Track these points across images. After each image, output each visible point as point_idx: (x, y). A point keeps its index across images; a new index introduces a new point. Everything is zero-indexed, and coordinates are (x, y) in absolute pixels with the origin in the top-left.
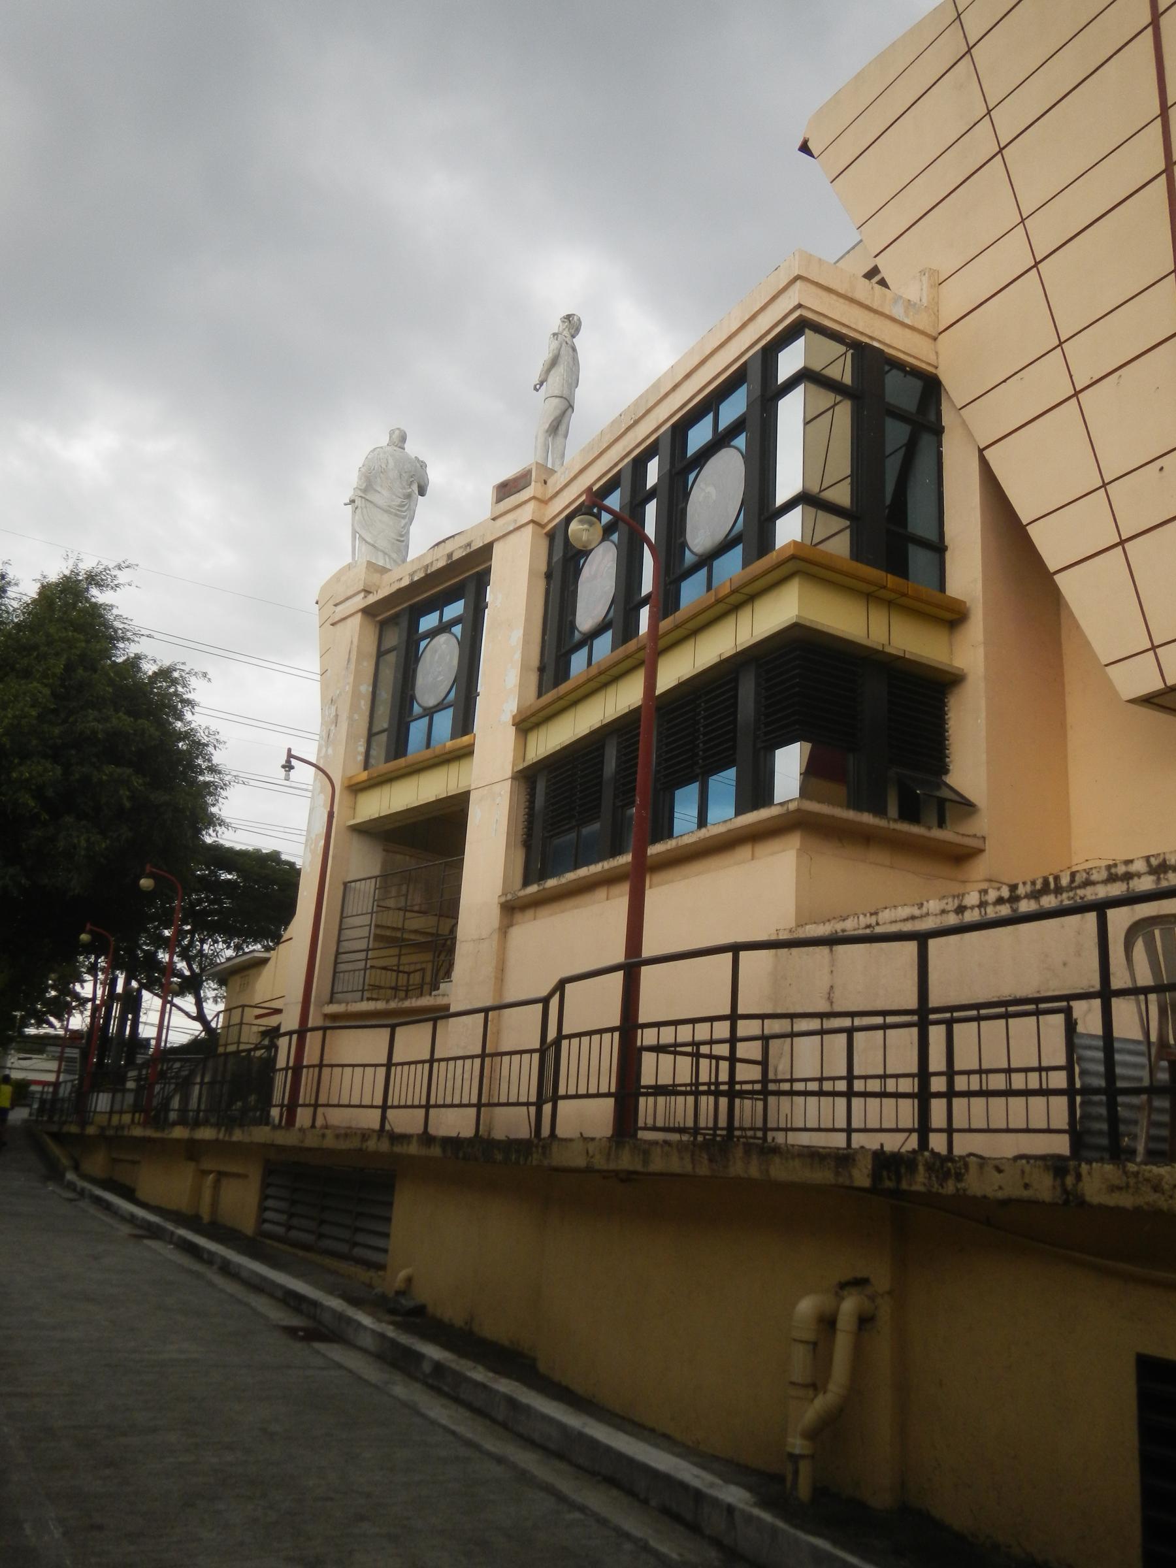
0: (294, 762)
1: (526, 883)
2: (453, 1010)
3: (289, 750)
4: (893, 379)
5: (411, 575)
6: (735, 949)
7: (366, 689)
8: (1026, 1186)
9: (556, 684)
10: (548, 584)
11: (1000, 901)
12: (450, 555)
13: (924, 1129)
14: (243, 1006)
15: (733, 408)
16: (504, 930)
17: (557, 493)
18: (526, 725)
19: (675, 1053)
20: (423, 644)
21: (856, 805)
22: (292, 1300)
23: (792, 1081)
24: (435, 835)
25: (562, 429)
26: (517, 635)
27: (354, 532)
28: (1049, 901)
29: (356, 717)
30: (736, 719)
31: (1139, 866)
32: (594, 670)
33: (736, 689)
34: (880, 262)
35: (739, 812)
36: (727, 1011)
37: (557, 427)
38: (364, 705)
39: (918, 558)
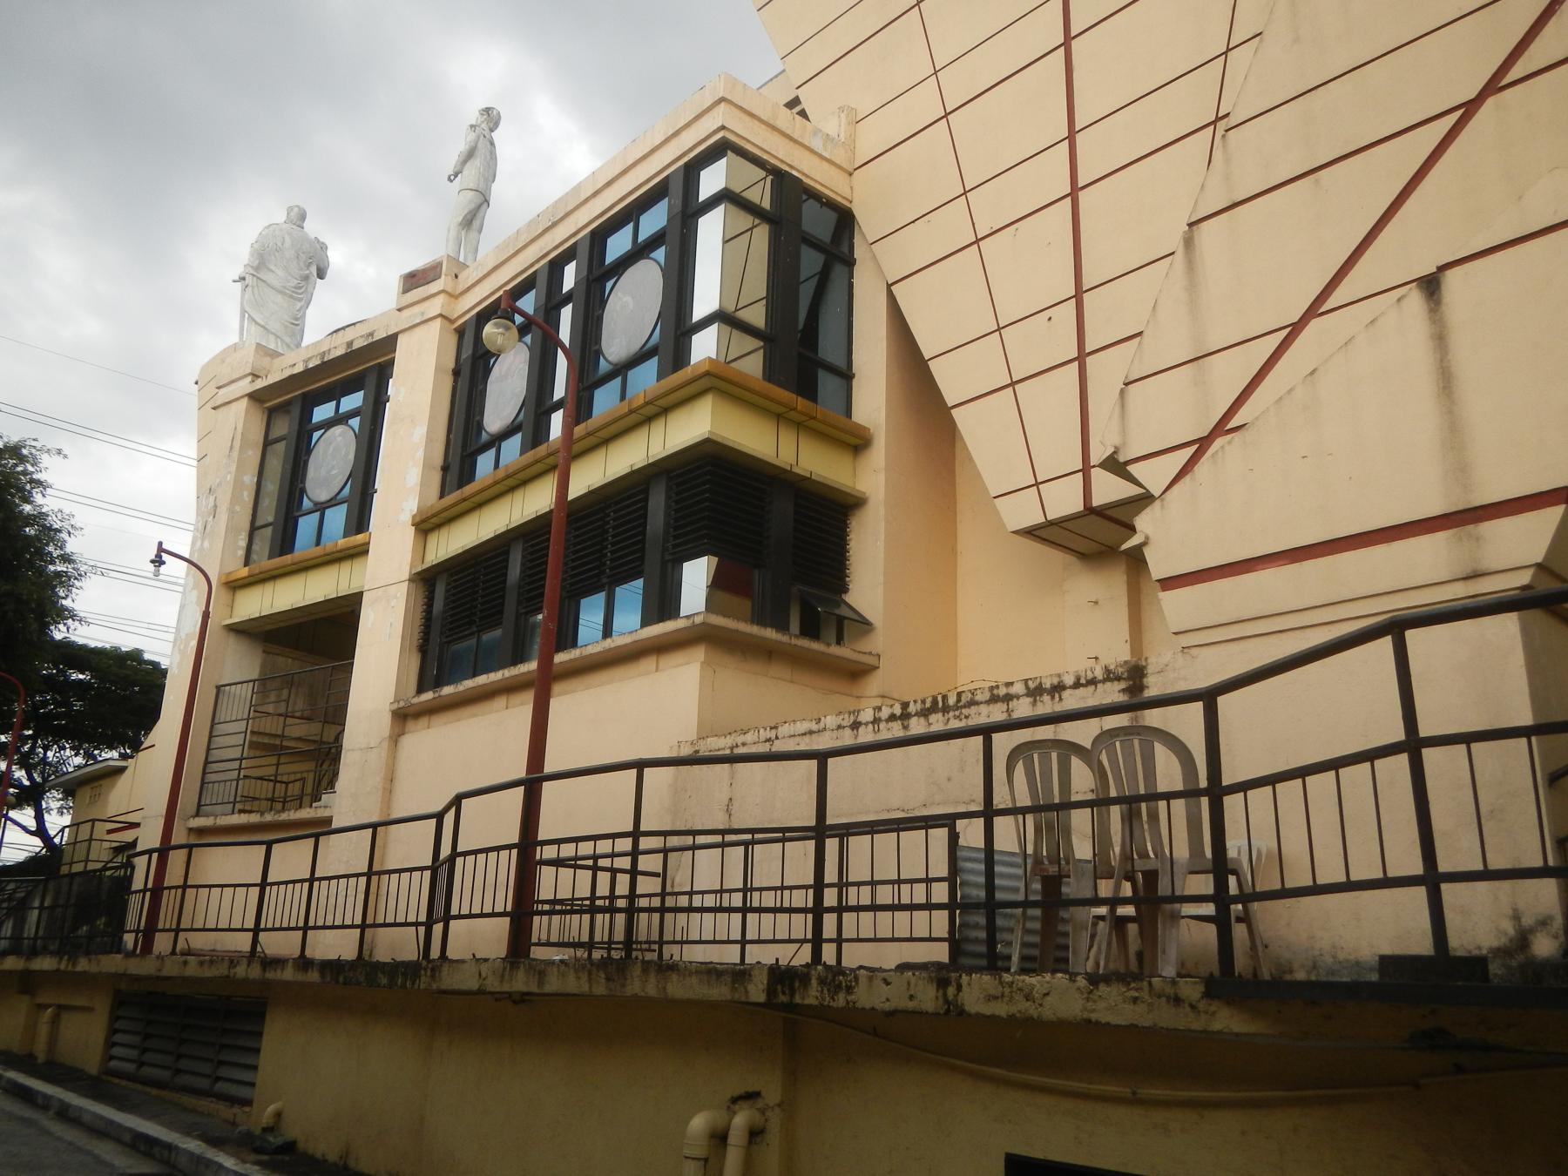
0: (165, 557)
1: (421, 690)
2: (335, 825)
3: (160, 544)
4: (809, 208)
5: (306, 361)
6: (640, 765)
7: (250, 479)
8: (911, 997)
9: (460, 486)
10: (455, 381)
11: (892, 718)
12: (350, 344)
13: (817, 941)
14: (93, 821)
15: (654, 220)
16: (395, 738)
17: (469, 289)
18: (426, 526)
19: (576, 867)
20: (316, 435)
21: (759, 618)
22: (142, 1145)
23: (691, 893)
24: (327, 635)
25: (476, 223)
26: (420, 432)
27: (243, 312)
28: (937, 723)
29: (238, 508)
30: (643, 533)
31: (1018, 688)
32: (501, 473)
33: (646, 500)
34: (801, 93)
35: (645, 622)
36: (630, 828)
37: (471, 220)
38: (248, 497)
39: (827, 384)
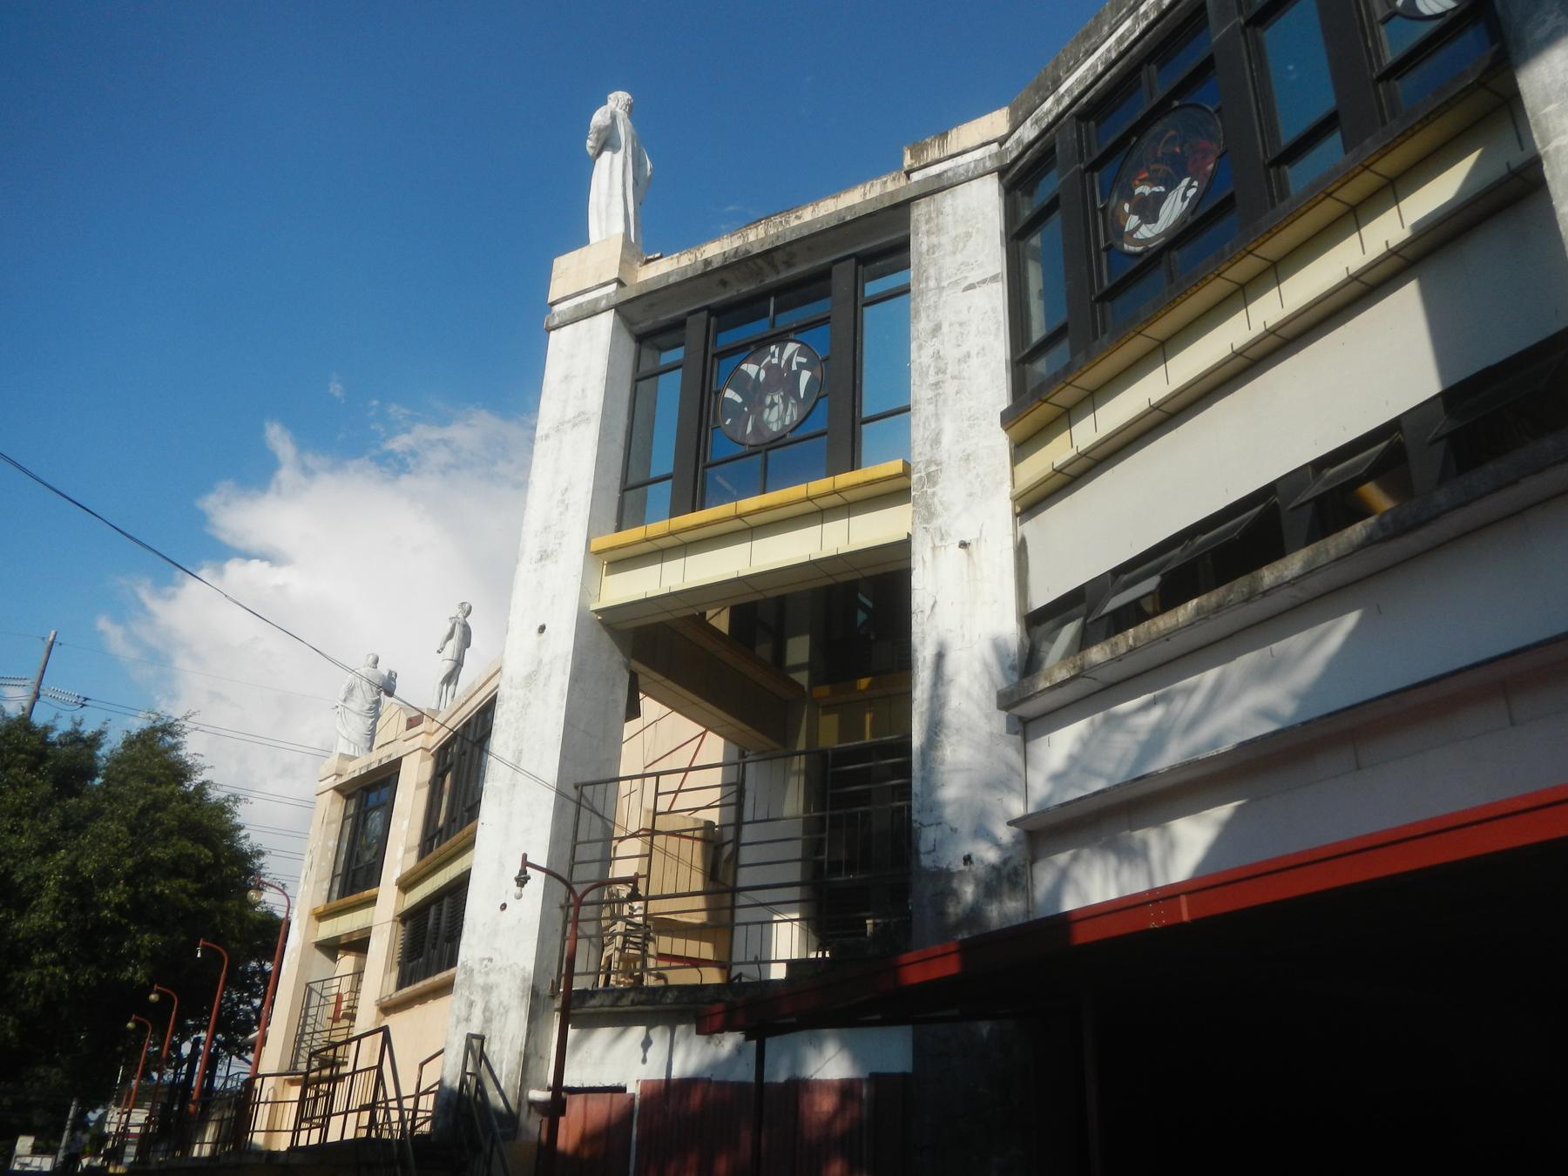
7: (333, 843)
18: (406, 885)
26: (406, 823)
